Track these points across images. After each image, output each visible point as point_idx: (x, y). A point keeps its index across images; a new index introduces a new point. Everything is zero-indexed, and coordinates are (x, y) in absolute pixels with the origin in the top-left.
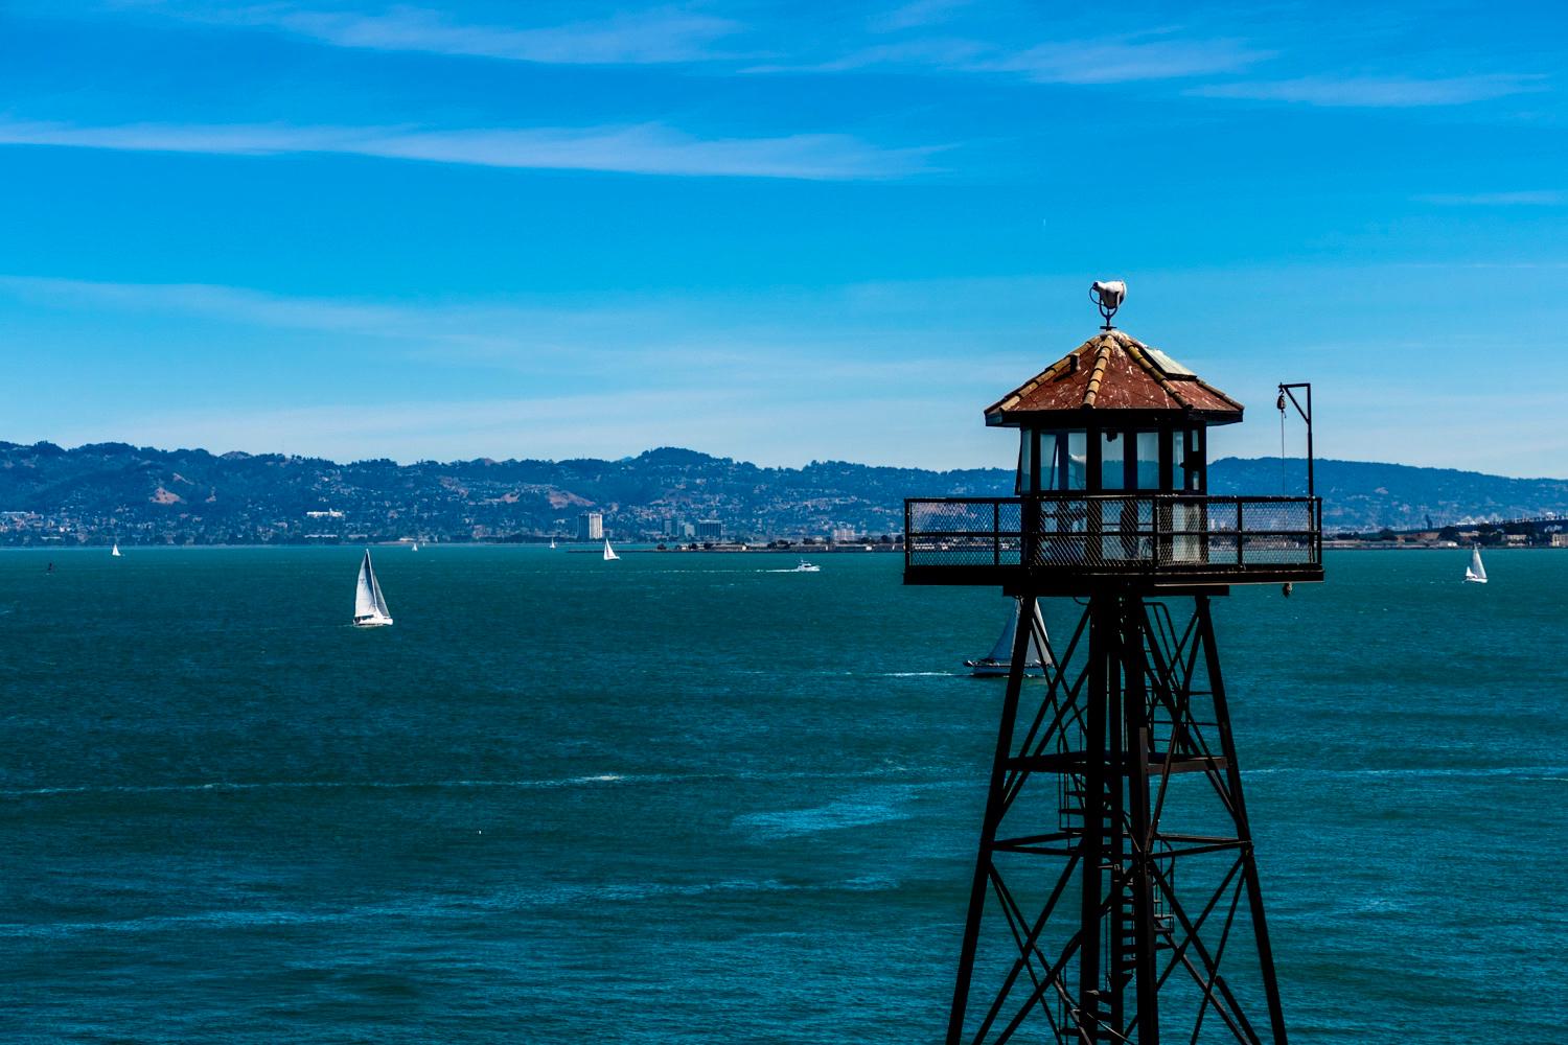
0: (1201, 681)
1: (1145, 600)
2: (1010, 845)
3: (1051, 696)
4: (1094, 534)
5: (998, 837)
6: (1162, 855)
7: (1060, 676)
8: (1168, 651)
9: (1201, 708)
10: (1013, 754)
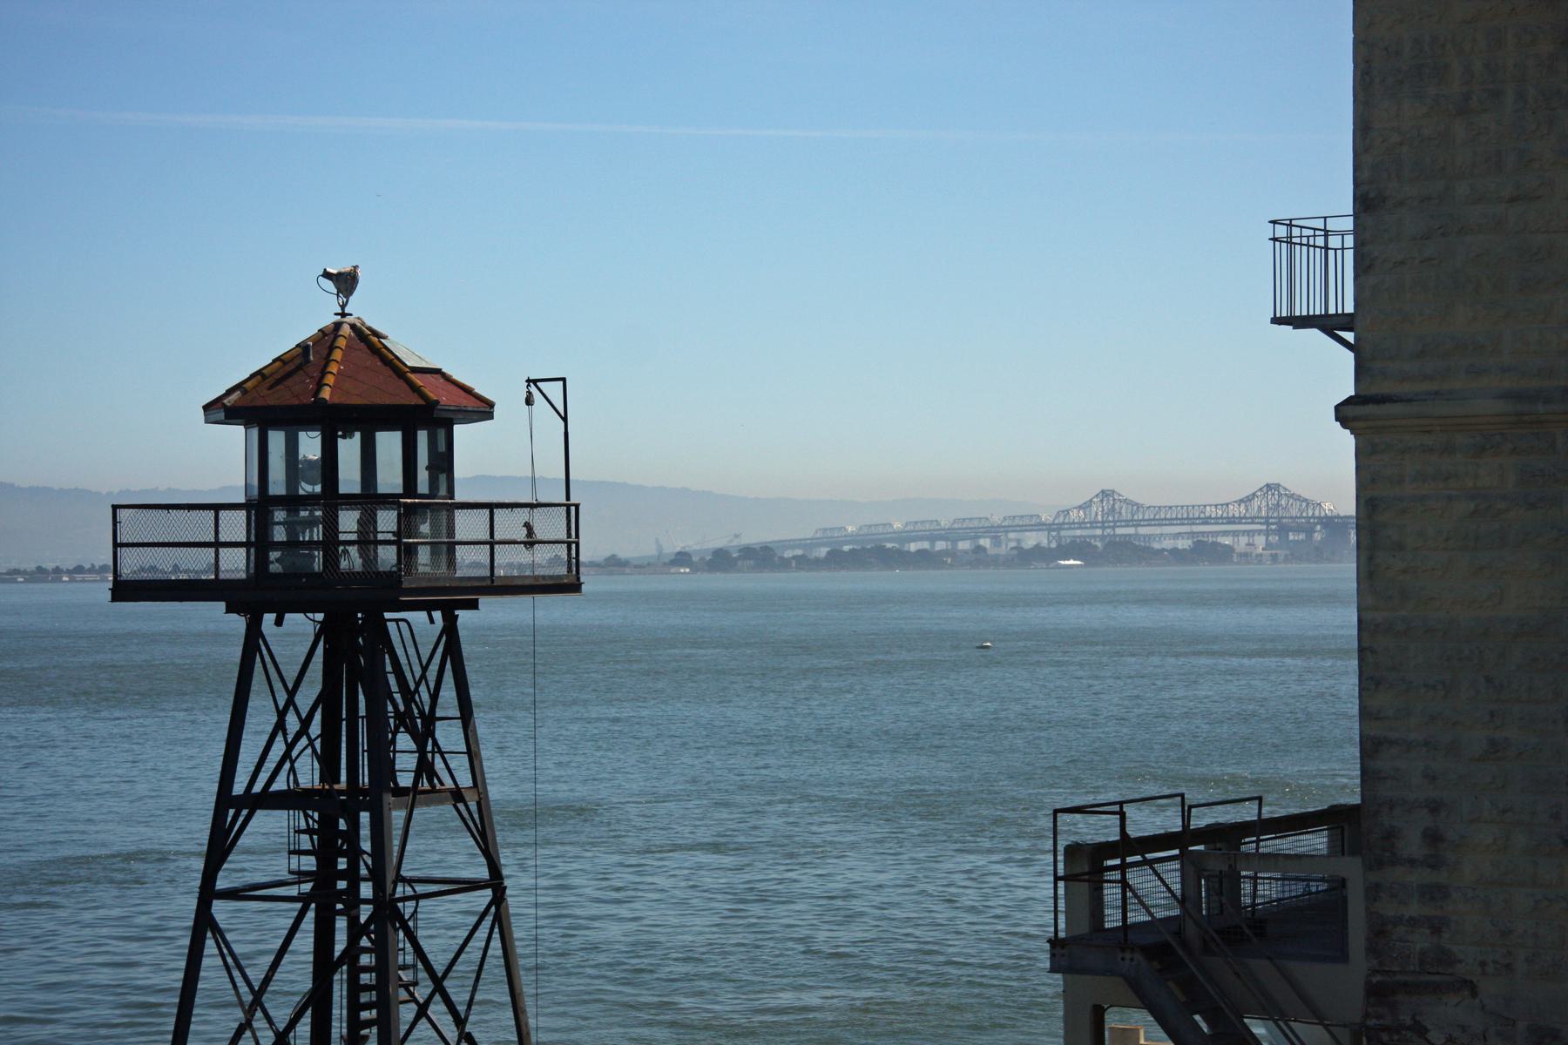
1: (387, 615)
2: (233, 894)
3: (280, 726)
4: (331, 543)
5: (222, 883)
6: (405, 899)
7: (290, 702)
8: (412, 673)
9: (449, 735)
10: (239, 788)
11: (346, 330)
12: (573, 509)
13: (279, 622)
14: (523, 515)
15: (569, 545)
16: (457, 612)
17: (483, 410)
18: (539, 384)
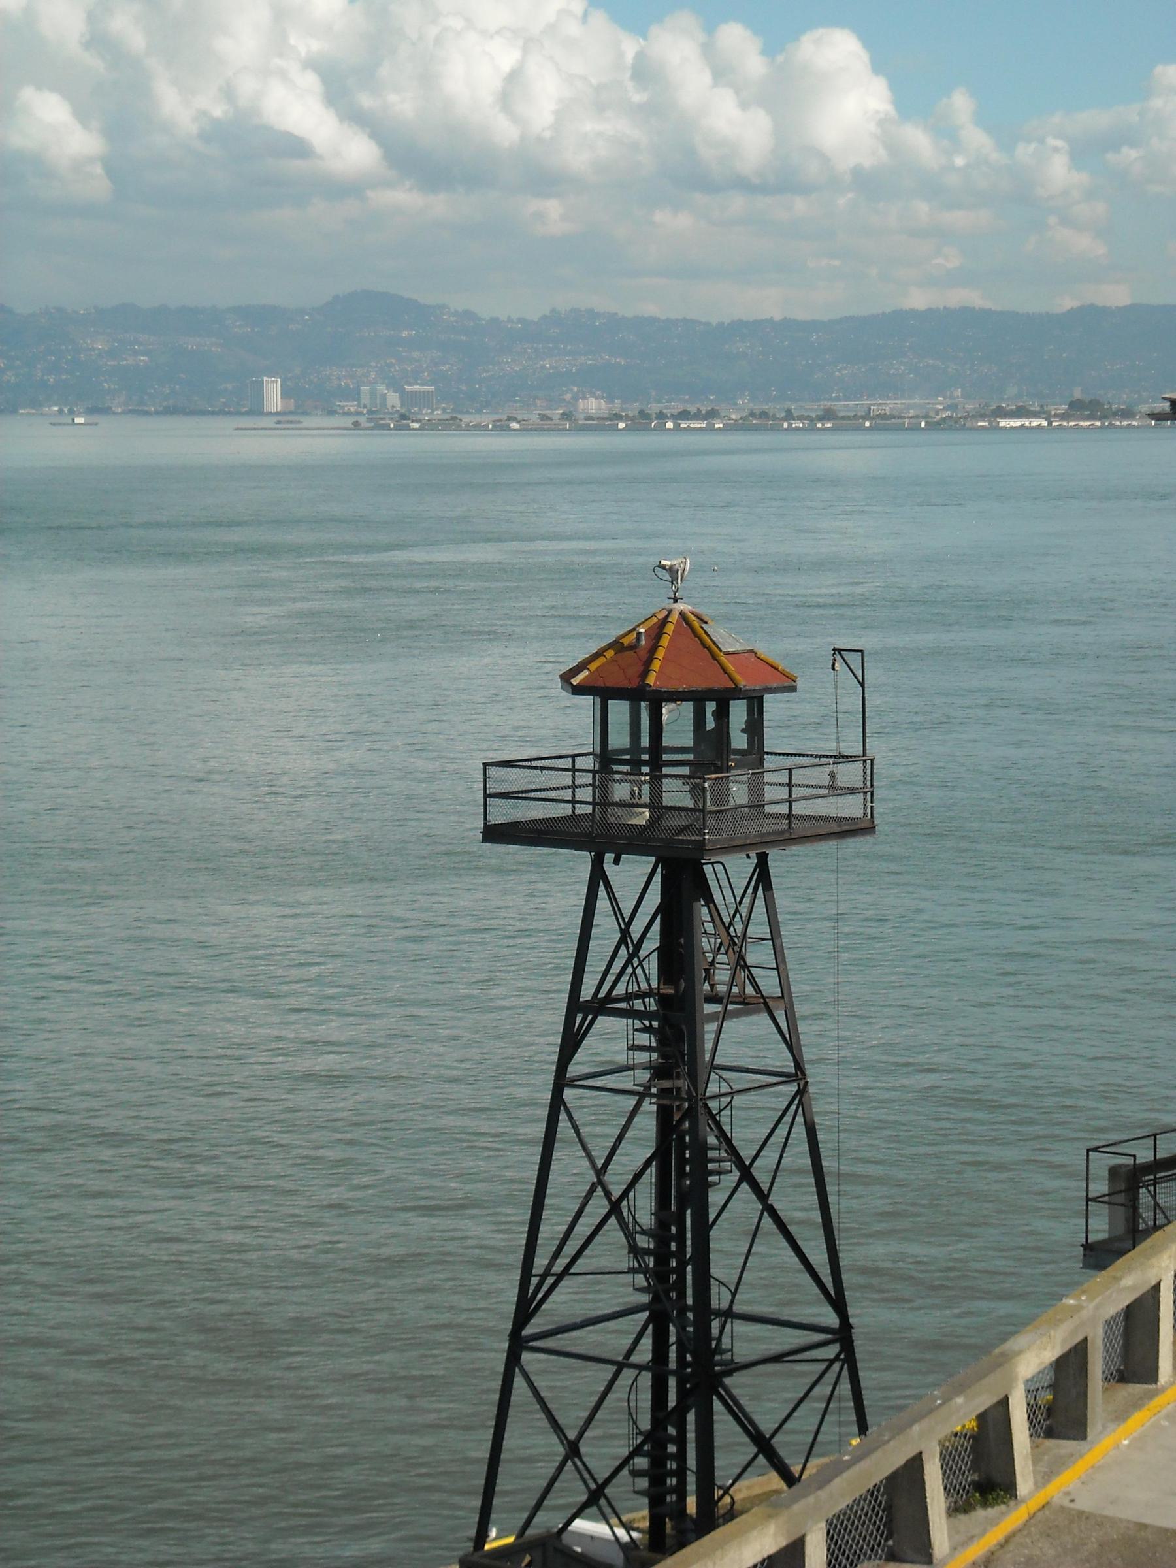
0: (759, 927)
5: (573, 1070)
10: (586, 994)
11: (674, 617)
12: (869, 762)
13: (617, 861)
15: (865, 793)
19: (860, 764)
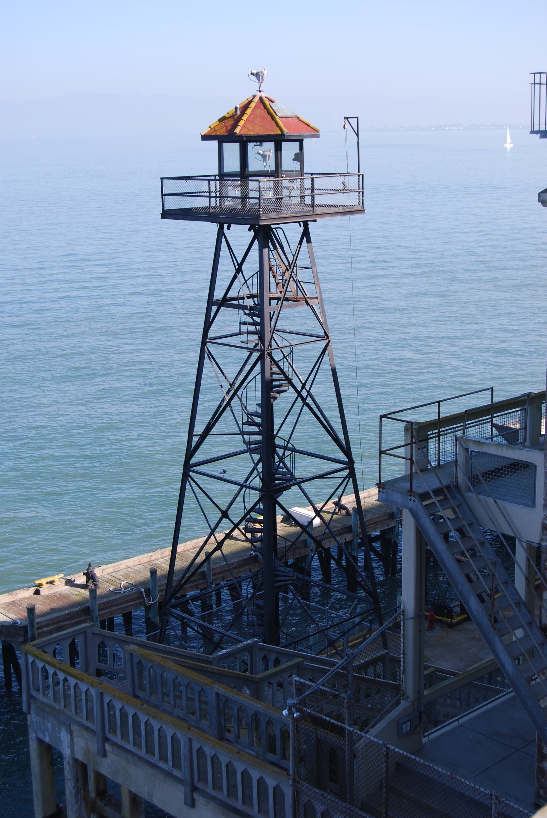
12: (361, 176)
14: (341, 179)
16: (308, 222)
17: (315, 133)
18: (349, 119)
19: (357, 177)
